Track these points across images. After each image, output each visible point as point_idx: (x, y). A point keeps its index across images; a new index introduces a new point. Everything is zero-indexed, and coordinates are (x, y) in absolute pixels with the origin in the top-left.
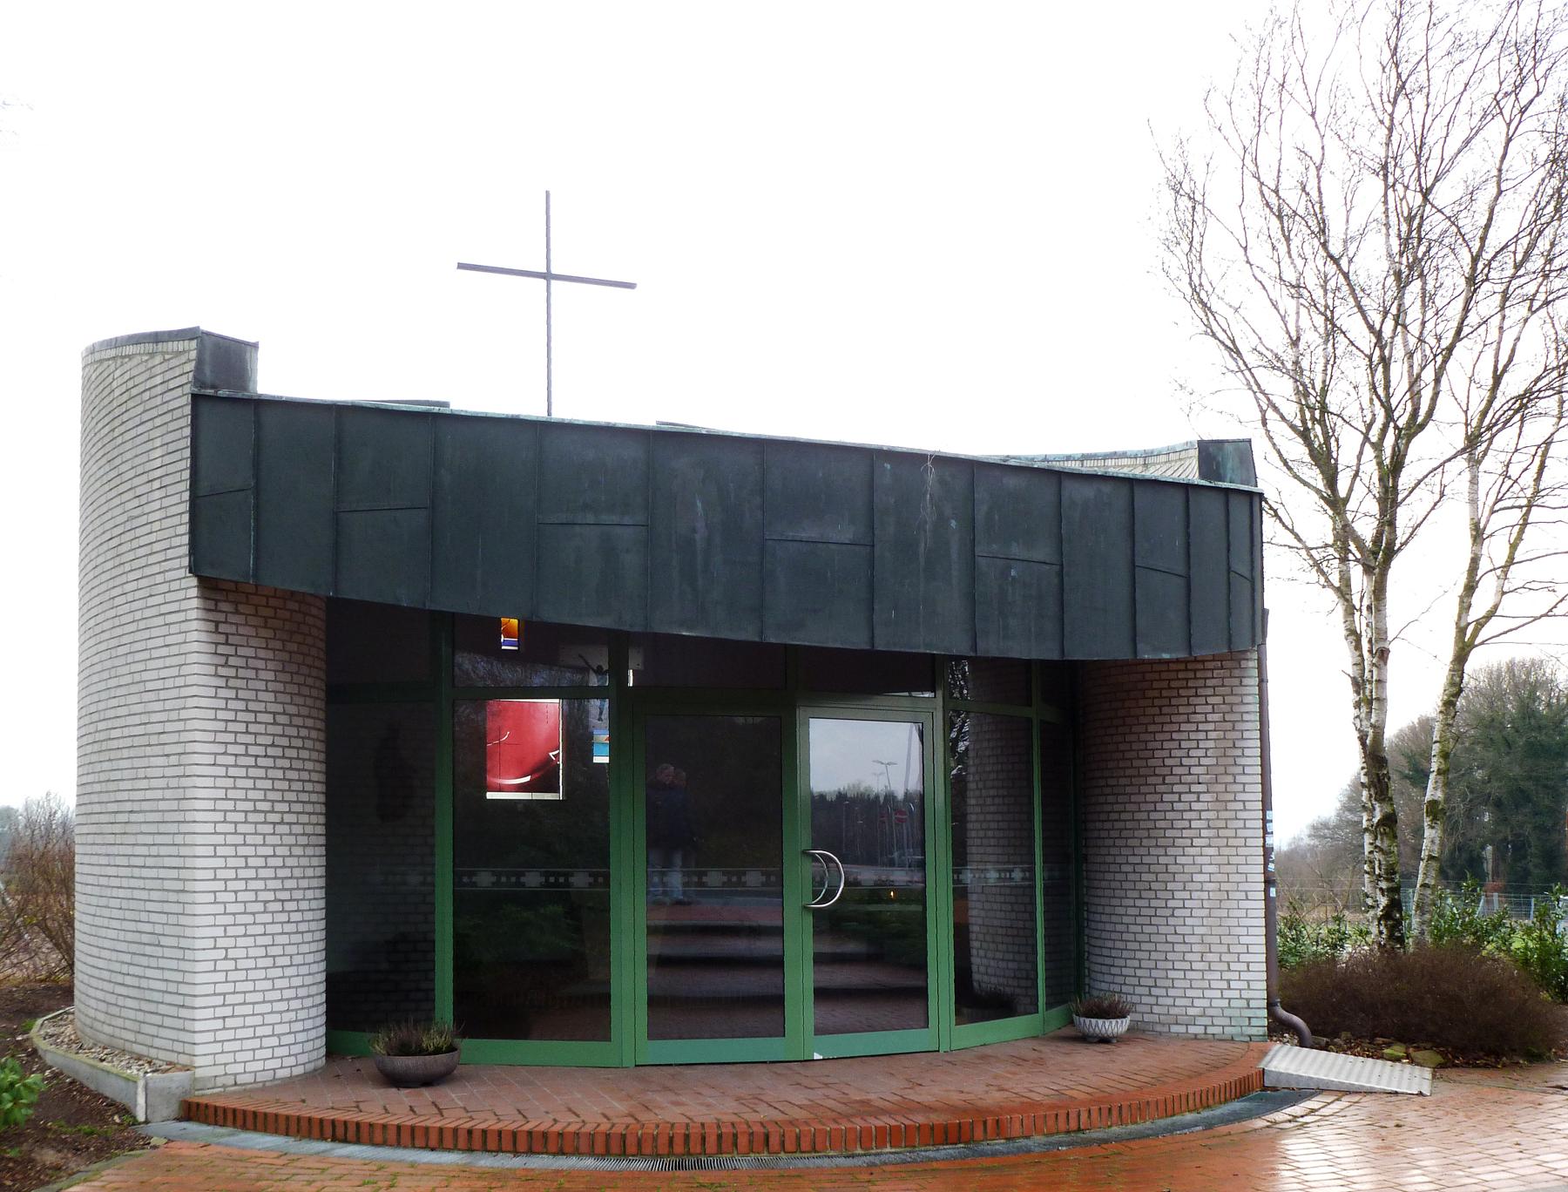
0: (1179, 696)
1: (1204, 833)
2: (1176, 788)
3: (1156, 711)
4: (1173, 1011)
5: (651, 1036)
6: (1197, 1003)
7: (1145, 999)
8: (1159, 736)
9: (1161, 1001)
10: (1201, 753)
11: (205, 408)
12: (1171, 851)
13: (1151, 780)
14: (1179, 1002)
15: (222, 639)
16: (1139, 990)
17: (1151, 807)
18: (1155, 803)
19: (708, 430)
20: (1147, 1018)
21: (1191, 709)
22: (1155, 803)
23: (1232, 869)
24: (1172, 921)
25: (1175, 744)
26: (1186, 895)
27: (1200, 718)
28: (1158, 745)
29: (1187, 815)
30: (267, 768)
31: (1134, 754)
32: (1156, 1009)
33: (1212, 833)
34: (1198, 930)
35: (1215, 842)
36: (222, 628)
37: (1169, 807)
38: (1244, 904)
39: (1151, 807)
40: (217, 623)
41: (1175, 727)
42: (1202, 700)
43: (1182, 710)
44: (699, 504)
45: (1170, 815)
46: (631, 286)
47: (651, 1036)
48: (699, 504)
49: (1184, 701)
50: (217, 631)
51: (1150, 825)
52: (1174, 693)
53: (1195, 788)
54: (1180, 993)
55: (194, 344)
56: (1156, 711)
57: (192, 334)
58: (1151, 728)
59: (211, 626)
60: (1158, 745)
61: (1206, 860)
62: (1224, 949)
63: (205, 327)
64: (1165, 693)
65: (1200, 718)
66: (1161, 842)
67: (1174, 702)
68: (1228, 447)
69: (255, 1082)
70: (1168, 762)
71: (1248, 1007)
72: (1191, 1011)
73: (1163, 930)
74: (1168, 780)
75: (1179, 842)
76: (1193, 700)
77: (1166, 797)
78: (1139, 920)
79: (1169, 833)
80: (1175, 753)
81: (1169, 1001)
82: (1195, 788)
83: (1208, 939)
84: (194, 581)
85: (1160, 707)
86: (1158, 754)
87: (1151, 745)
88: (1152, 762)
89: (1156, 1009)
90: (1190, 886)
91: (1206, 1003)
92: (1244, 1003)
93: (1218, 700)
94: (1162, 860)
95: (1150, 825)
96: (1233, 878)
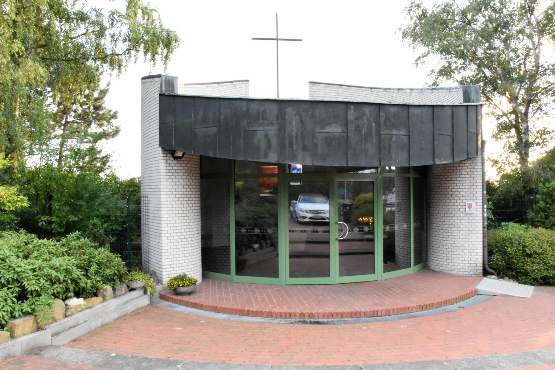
2: (456, 198)
4: (453, 267)
8: (450, 182)
12: (453, 218)
13: (448, 196)
15: (168, 165)
16: (443, 260)
20: (445, 269)
24: (453, 239)
25: (455, 185)
26: (458, 232)
36: (168, 162)
40: (167, 160)
42: (464, 170)
50: (167, 163)
54: (455, 261)
59: (165, 161)
70: (453, 190)
71: (477, 266)
72: (459, 267)
73: (450, 242)
74: (453, 196)
76: (461, 171)
77: (453, 201)
80: (455, 187)
84: (160, 149)
86: (450, 187)
87: (448, 185)
88: (448, 190)
89: (448, 266)
91: (463, 265)
92: (475, 265)
93: (469, 170)
94: (451, 221)
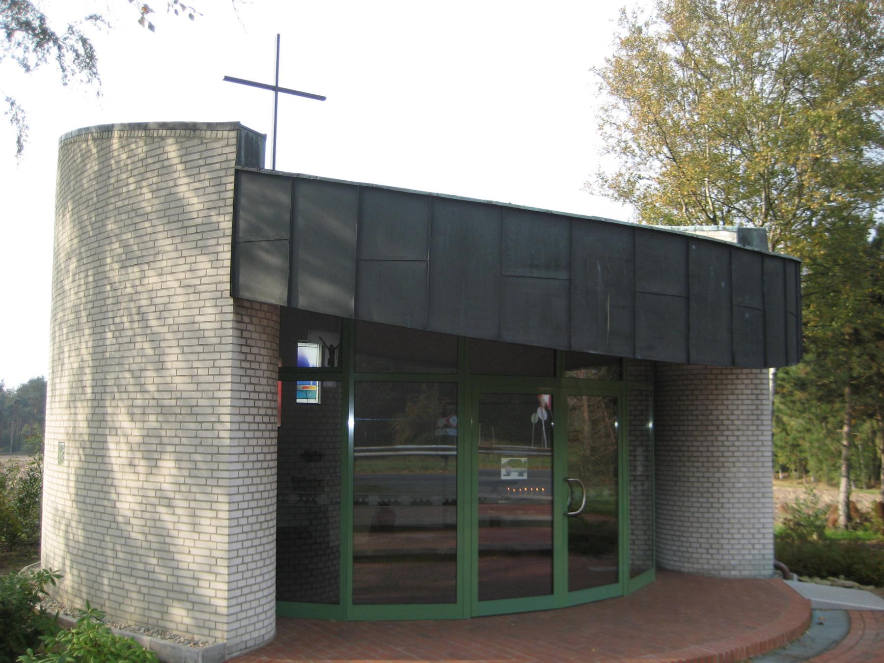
0: (727, 379)
1: (741, 459)
2: (726, 433)
3: (714, 387)
4: (723, 562)
5: (481, 599)
6: (736, 557)
7: (704, 556)
8: (715, 402)
9: (715, 557)
10: (739, 412)
11: (244, 179)
12: (722, 470)
13: (710, 428)
14: (726, 557)
15: (243, 342)
16: (700, 550)
17: (710, 444)
18: (712, 441)
19: (605, 219)
20: (705, 567)
21: (734, 387)
22: (712, 441)
23: (755, 480)
24: (722, 510)
25: (724, 407)
26: (730, 495)
27: (739, 392)
28: (714, 407)
29: (732, 449)
30: (758, 462)
31: (698, 412)
32: (712, 562)
33: (745, 459)
34: (737, 516)
35: (747, 464)
36: (245, 334)
37: (720, 444)
38: (763, 500)
39: (710, 444)
40: (242, 331)
41: (725, 397)
42: (740, 382)
43: (729, 387)
44: (599, 267)
45: (722, 449)
46: (227, 79)
47: (481, 599)
48: (599, 267)
49: (729, 382)
50: (242, 337)
51: (689, 454)
52: (724, 377)
53: (736, 433)
54: (726, 552)
55: (233, 134)
56: (714, 387)
57: (236, 127)
58: (711, 397)
59: (238, 333)
60: (714, 407)
61: (742, 475)
62: (751, 526)
63: (244, 123)
64: (719, 377)
65: (739, 392)
66: (716, 464)
67: (724, 382)
68: (755, 234)
69: (246, 648)
70: (721, 417)
71: (764, 559)
72: (733, 562)
73: (716, 515)
74: (721, 428)
75: (726, 464)
76: (736, 382)
77: (720, 438)
78: (701, 510)
79: (721, 459)
80: (725, 412)
81: (720, 557)
82: (736, 433)
83: (742, 521)
84: (231, 301)
85: (716, 385)
86: (715, 412)
87: (710, 407)
88: (711, 417)
89: (712, 562)
90: (733, 490)
91: (740, 557)
92: (761, 557)
93: (748, 381)
94: (717, 475)
95: (689, 454)
96: (757, 485)
